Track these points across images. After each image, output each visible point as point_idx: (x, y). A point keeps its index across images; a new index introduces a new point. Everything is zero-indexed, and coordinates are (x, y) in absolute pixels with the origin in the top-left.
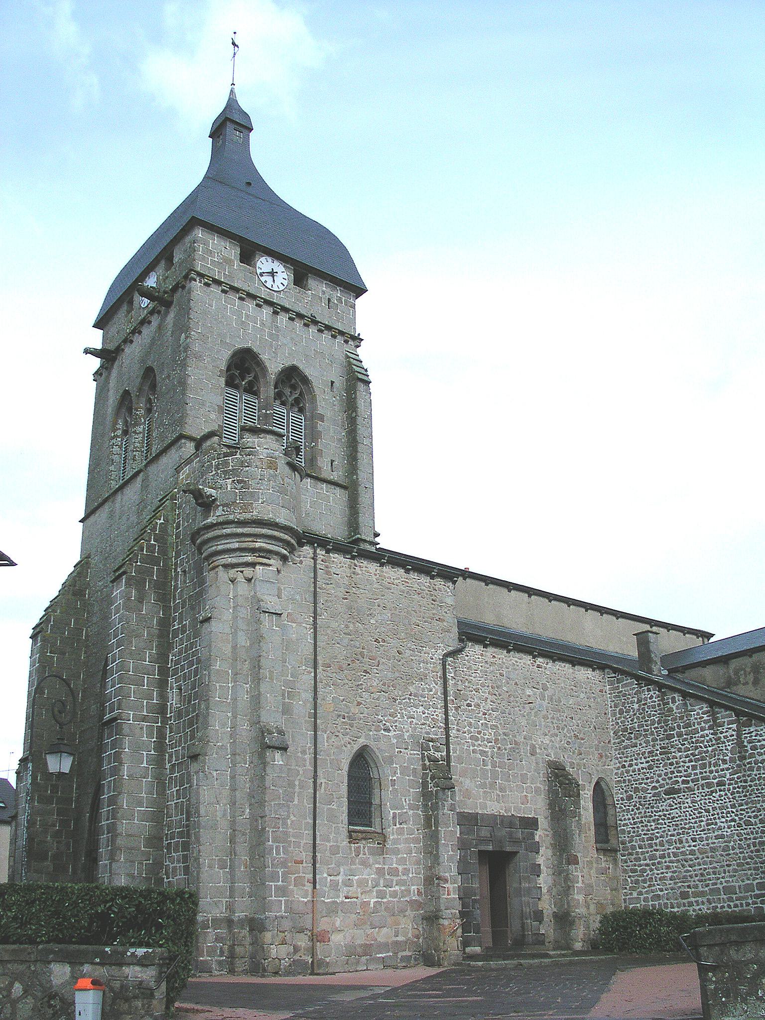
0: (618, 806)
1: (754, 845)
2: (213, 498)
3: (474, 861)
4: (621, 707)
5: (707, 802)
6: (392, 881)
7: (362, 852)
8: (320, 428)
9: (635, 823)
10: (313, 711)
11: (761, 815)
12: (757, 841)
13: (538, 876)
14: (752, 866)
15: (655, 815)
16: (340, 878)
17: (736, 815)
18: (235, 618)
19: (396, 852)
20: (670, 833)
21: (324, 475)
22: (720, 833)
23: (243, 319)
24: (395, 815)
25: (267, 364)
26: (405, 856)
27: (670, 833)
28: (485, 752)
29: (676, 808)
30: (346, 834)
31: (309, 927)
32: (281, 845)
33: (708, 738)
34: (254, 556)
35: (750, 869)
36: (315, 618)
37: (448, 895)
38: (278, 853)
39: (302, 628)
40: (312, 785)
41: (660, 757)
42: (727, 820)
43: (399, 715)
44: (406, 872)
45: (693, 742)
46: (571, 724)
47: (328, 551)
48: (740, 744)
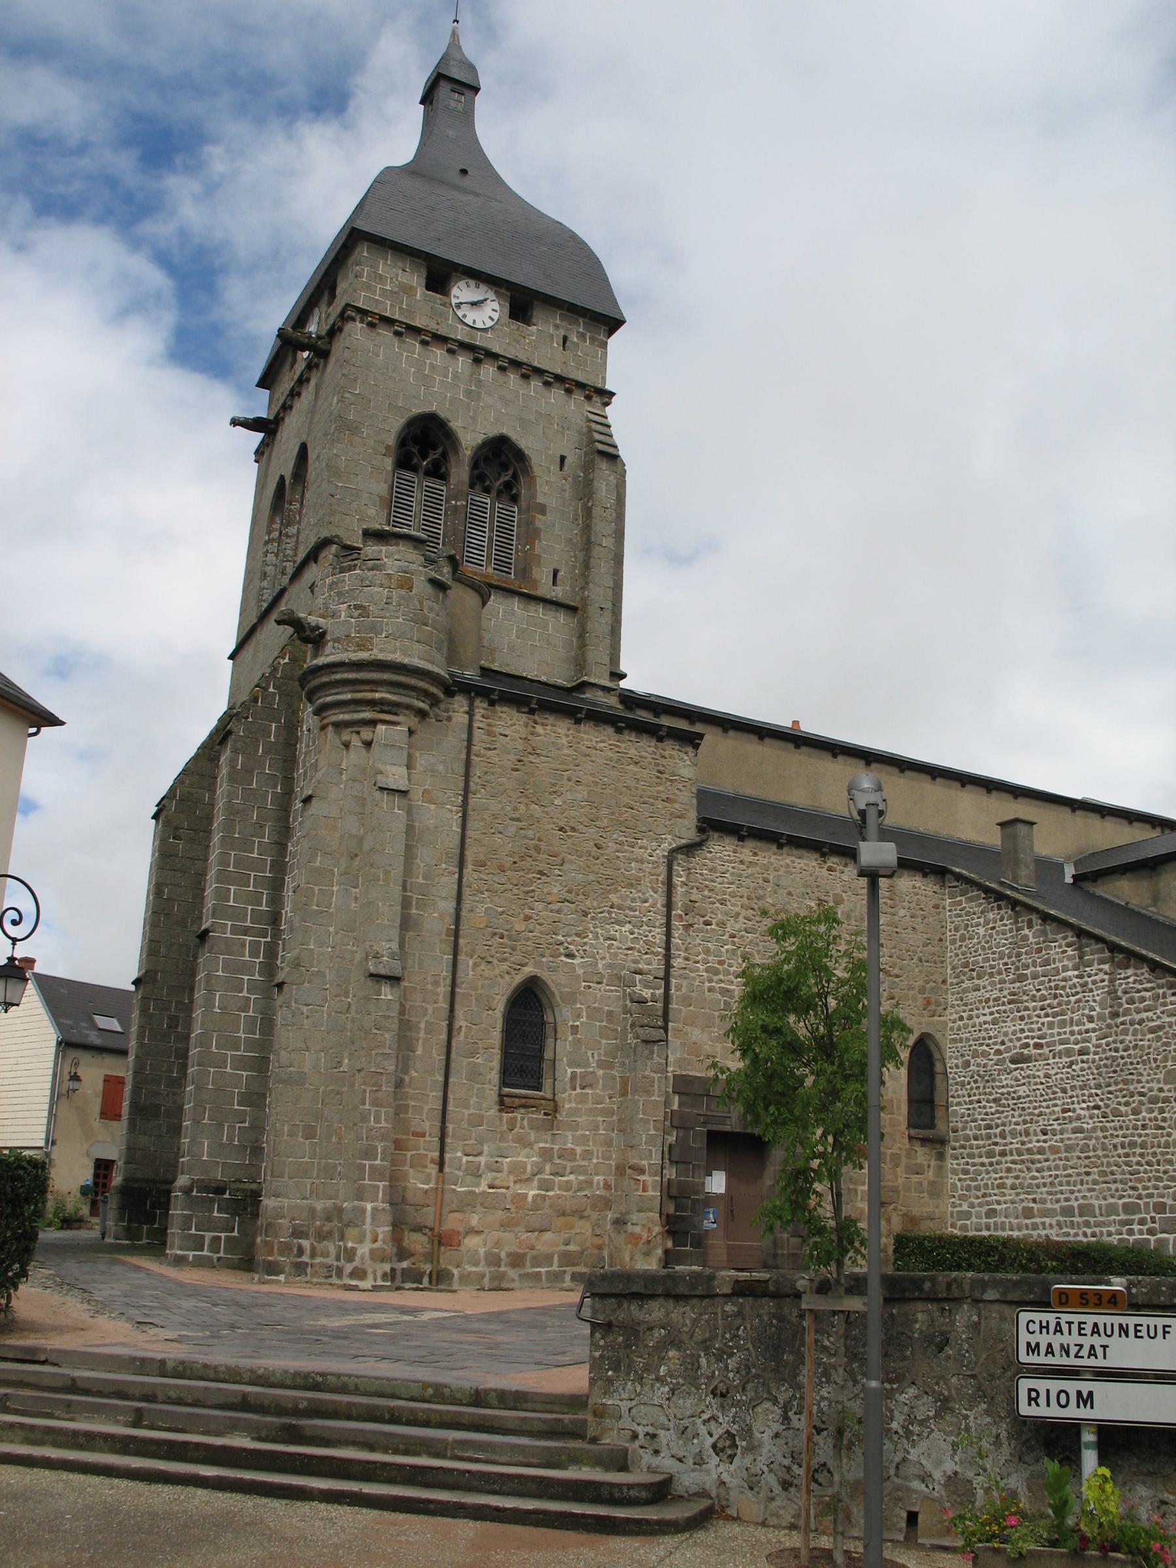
3: (701, 1143)
4: (962, 932)
6: (565, 1168)
7: (518, 1125)
8: (538, 524)
9: (971, 1102)
10: (453, 927)
11: (1134, 1102)
12: (1127, 1140)
15: (997, 1093)
16: (482, 1160)
17: (1102, 1100)
19: (575, 1126)
20: (1014, 1120)
21: (540, 592)
24: (574, 1075)
26: (587, 1133)
27: (1014, 1120)
28: (728, 990)
29: (1024, 1084)
30: (495, 1098)
31: (429, 1223)
32: (383, 1110)
35: (1115, 1182)
37: (644, 1191)
38: (377, 1121)
40: (445, 1030)
41: (1008, 1007)
42: (1088, 1106)
43: (591, 936)
44: (587, 1155)
47: (492, 703)
48: (1112, 993)
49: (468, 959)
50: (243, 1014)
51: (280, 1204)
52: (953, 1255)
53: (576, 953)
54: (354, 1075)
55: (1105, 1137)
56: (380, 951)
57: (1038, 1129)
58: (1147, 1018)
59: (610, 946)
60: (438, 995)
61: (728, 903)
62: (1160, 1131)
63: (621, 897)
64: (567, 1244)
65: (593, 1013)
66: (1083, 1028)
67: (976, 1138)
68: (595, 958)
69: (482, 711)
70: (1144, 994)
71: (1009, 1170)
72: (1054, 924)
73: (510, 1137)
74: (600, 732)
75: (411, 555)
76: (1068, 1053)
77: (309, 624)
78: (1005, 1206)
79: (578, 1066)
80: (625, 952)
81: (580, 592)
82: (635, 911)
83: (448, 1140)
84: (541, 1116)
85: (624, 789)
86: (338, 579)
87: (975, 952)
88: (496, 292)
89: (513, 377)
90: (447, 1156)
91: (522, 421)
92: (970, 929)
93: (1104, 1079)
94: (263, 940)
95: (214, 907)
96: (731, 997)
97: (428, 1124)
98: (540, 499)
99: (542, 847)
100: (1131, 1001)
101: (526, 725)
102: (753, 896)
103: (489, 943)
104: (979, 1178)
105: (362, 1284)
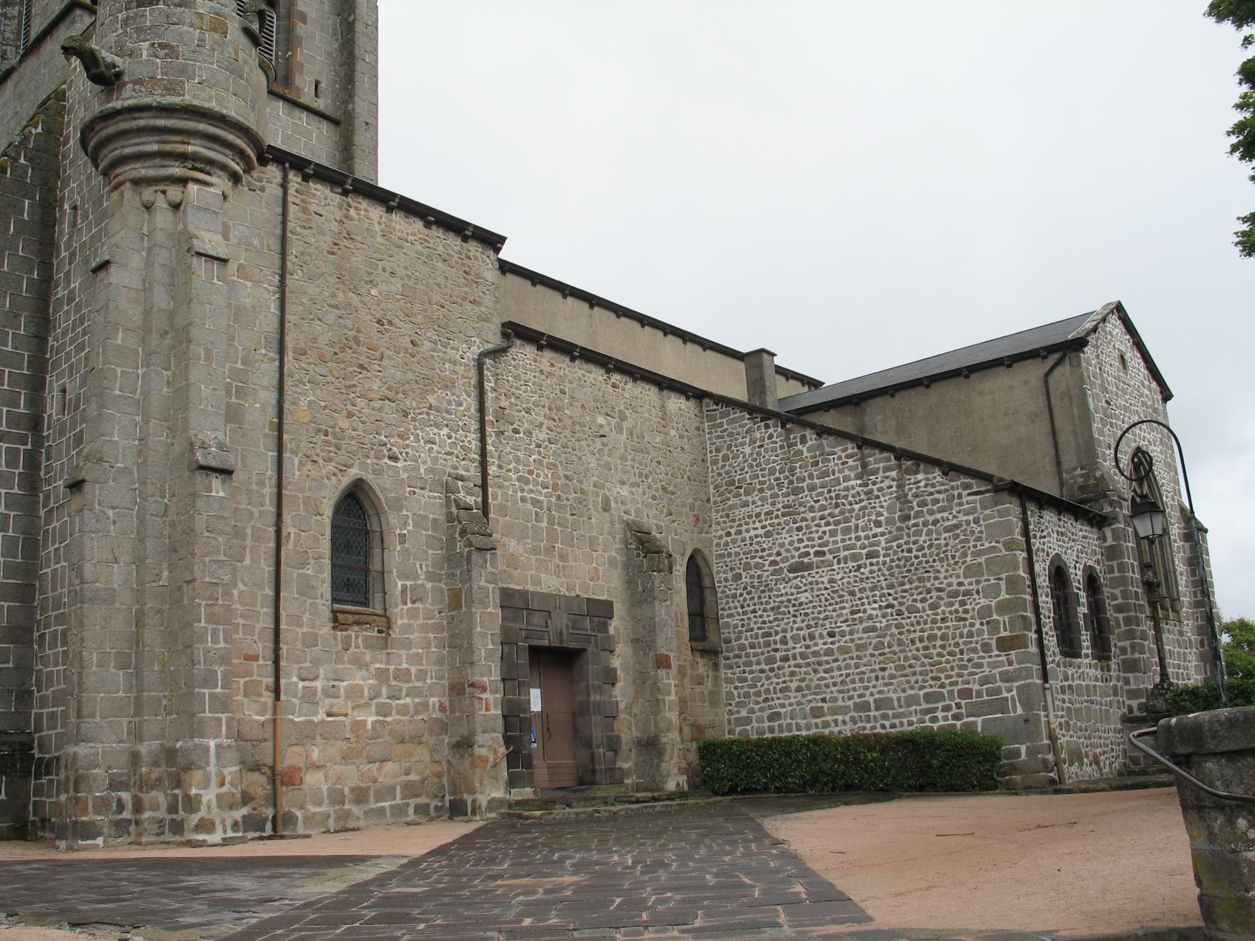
0: (720, 590)
1: (921, 640)
3: (524, 659)
4: (725, 452)
5: (852, 580)
6: (401, 690)
7: (353, 644)
10: (276, 420)
11: (931, 598)
12: (926, 634)
13: (613, 685)
14: (918, 669)
15: (774, 601)
16: (318, 684)
17: (895, 599)
18: (149, 264)
19: (408, 644)
20: (796, 626)
21: (303, 100)
22: (870, 623)
26: (420, 651)
27: (796, 626)
30: (328, 614)
31: (269, 761)
32: (221, 628)
33: (854, 492)
35: (914, 674)
36: (283, 277)
37: (487, 710)
38: (215, 641)
40: (273, 537)
41: (782, 520)
42: (880, 606)
43: (412, 437)
45: (831, 498)
46: (658, 471)
47: (306, 178)
48: (902, 498)
52: (762, 757)
54: (180, 588)
55: (901, 633)
56: (206, 440)
57: (825, 633)
58: (943, 519)
59: (431, 450)
62: (962, 623)
64: (408, 774)
65: (419, 520)
66: (871, 534)
67: (752, 646)
69: (297, 186)
70: (936, 496)
71: (793, 674)
72: (831, 438)
73: (346, 659)
74: (411, 225)
76: (855, 557)
78: (790, 708)
79: (408, 578)
81: (343, 106)
83: (282, 663)
84: (375, 634)
85: (435, 287)
87: (741, 470)
90: (283, 681)
92: (733, 448)
93: (897, 578)
94: (22, 447)
96: (541, 508)
97: (260, 645)
99: (362, 339)
100: (923, 504)
103: (314, 440)
104: (759, 684)
105: (211, 838)
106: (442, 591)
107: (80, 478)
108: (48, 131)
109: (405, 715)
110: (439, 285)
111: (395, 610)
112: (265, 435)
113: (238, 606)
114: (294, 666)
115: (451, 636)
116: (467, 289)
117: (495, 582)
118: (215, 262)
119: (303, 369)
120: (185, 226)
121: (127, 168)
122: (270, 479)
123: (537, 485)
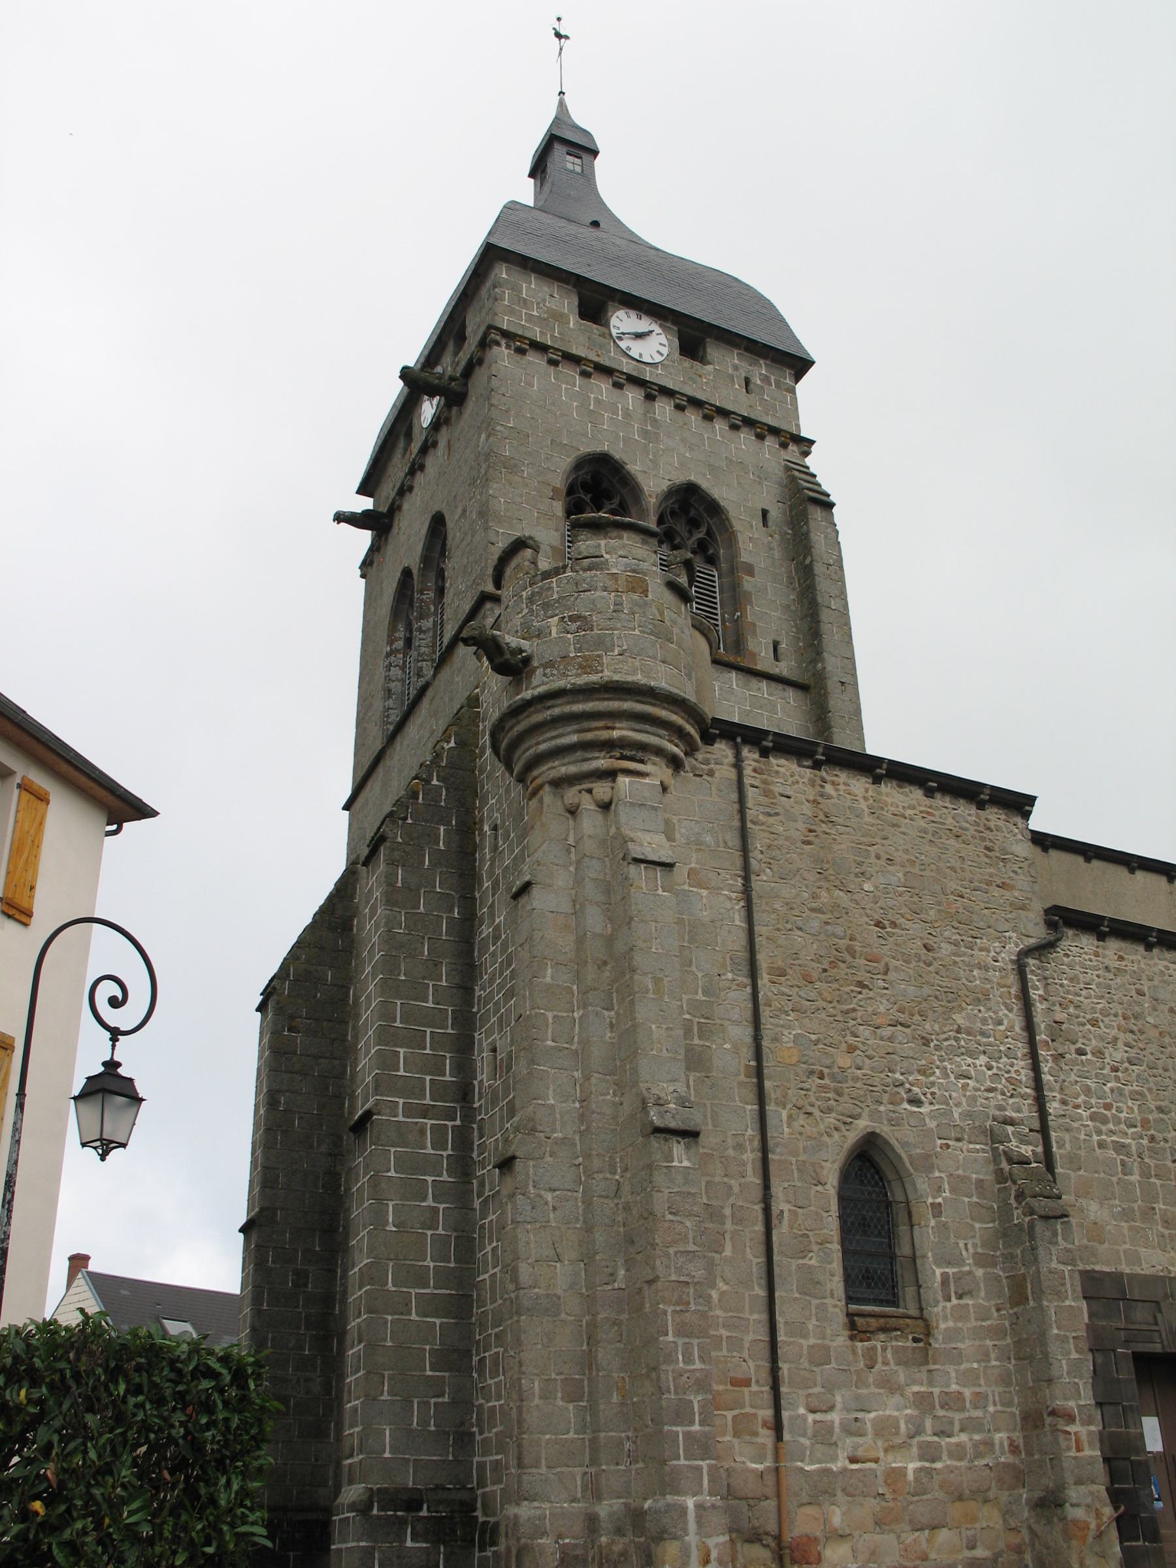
2: (524, 654)
3: (1127, 1373)
6: (951, 1423)
7: (880, 1359)
10: (753, 1063)
16: (835, 1417)
18: (579, 881)
19: (957, 1357)
21: (759, 667)
23: (592, 407)
25: (641, 479)
26: (975, 1365)
28: (1123, 1146)
30: (842, 1319)
31: (772, 1527)
32: (695, 1341)
34: (611, 757)
36: (746, 879)
38: (688, 1360)
39: (722, 898)
43: (937, 1071)
47: (765, 753)
49: (780, 1109)
50: (429, 1233)
51: (538, 1512)
53: (923, 1098)
54: (640, 1289)
56: (662, 1095)
60: (744, 1164)
61: (1101, 1024)
63: (968, 1017)
65: (958, 1183)
68: (948, 1104)
73: (871, 1380)
74: (907, 795)
75: (640, 551)
77: (507, 644)
79: (949, 1264)
80: (985, 1094)
81: (811, 667)
82: (989, 1037)
84: (910, 1344)
85: (948, 871)
86: (541, 588)
88: (661, 326)
89: (693, 417)
90: (785, 1414)
91: (712, 468)
94: (450, 1124)
95: (377, 1078)
96: (1128, 1155)
97: (751, 1364)
98: (745, 557)
99: (858, 949)
101: (812, 783)
102: (1129, 1013)
106: (997, 1279)
107: (510, 1154)
108: (461, 744)
109: (960, 1459)
110: (952, 868)
111: (935, 1309)
112: (741, 1084)
113: (718, 1312)
114: (800, 1392)
115: (1018, 1343)
116: (992, 870)
117: (1072, 1262)
118: (658, 869)
119: (783, 994)
120: (618, 829)
121: (544, 768)
122: (751, 1141)
123: (1120, 1123)
